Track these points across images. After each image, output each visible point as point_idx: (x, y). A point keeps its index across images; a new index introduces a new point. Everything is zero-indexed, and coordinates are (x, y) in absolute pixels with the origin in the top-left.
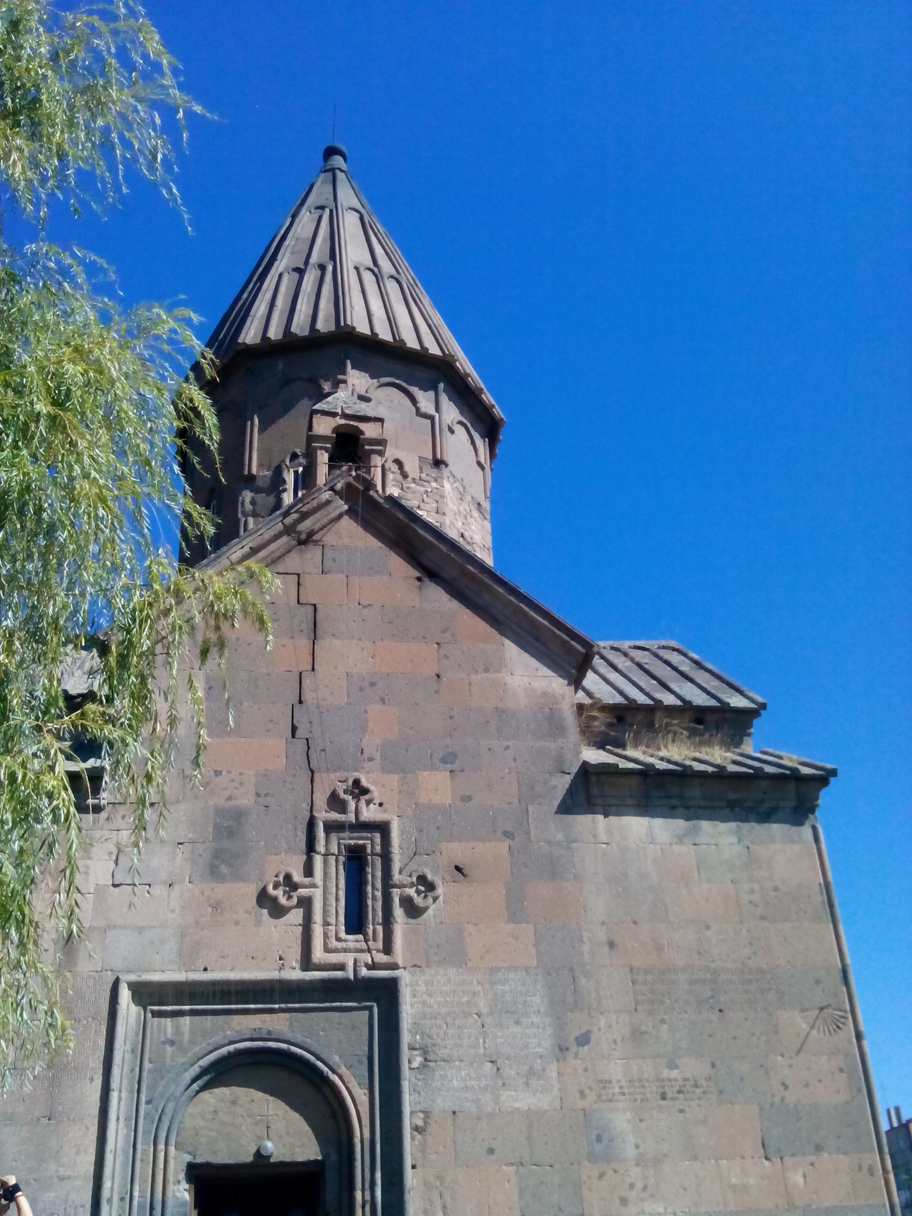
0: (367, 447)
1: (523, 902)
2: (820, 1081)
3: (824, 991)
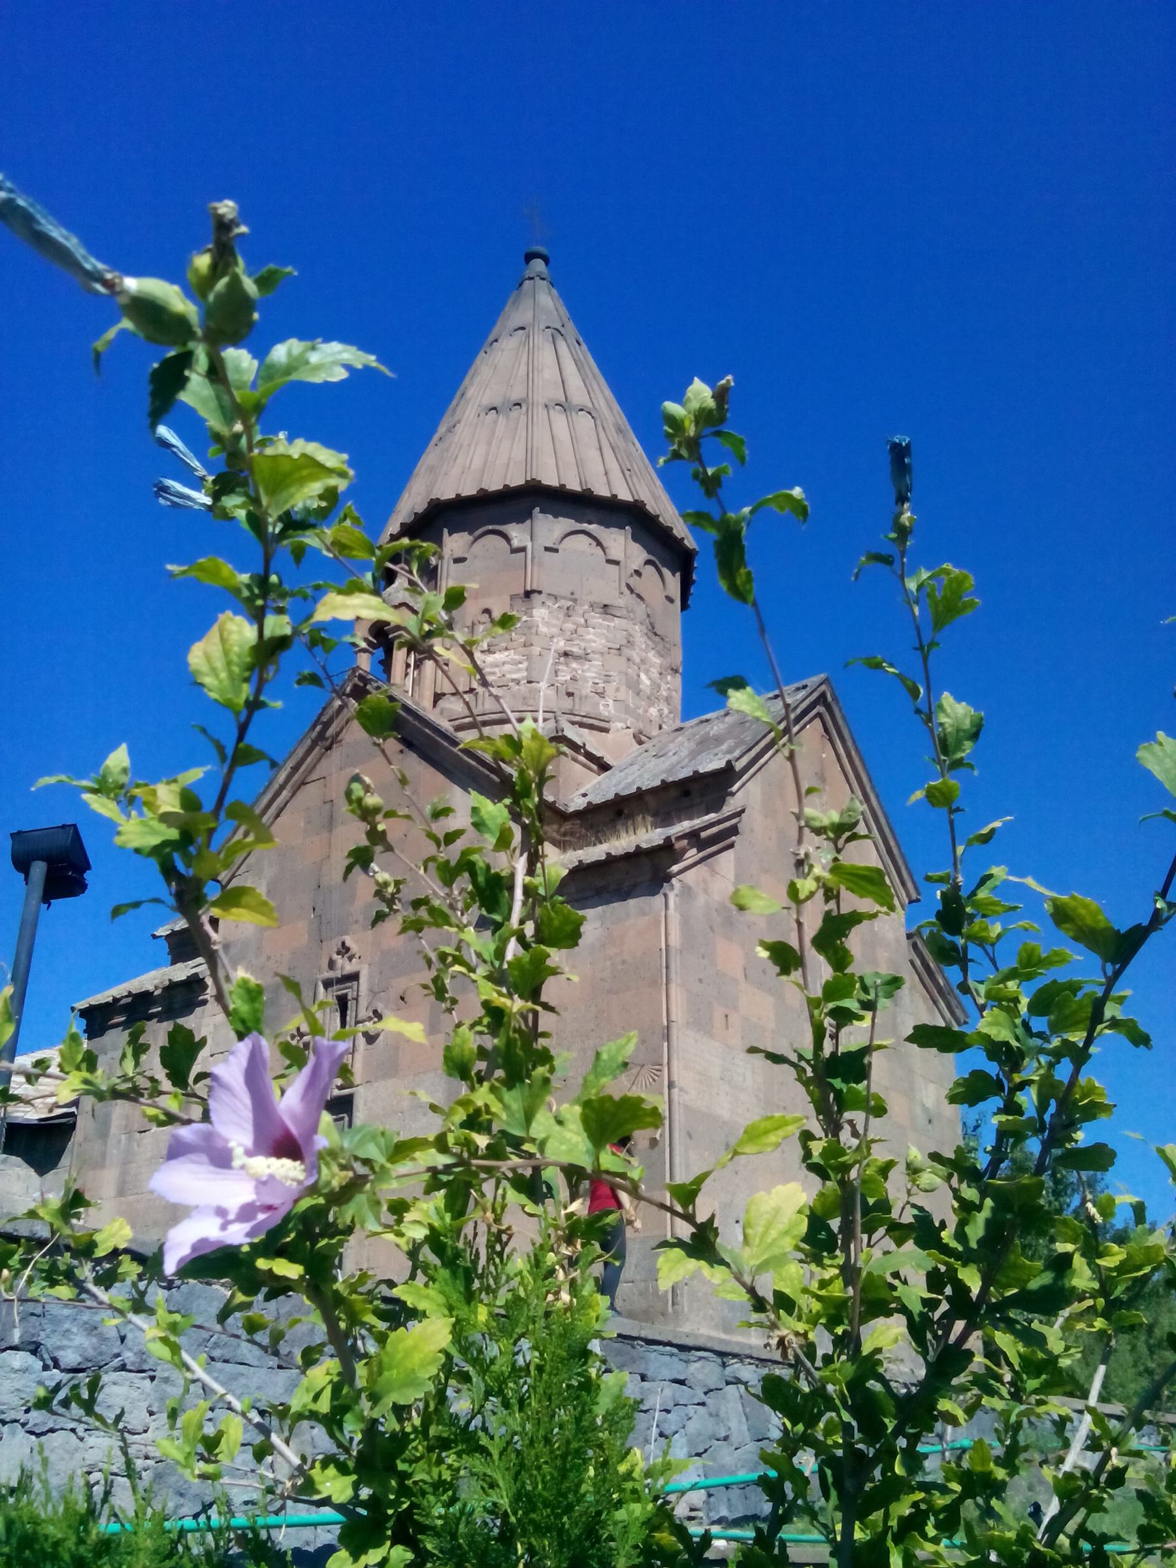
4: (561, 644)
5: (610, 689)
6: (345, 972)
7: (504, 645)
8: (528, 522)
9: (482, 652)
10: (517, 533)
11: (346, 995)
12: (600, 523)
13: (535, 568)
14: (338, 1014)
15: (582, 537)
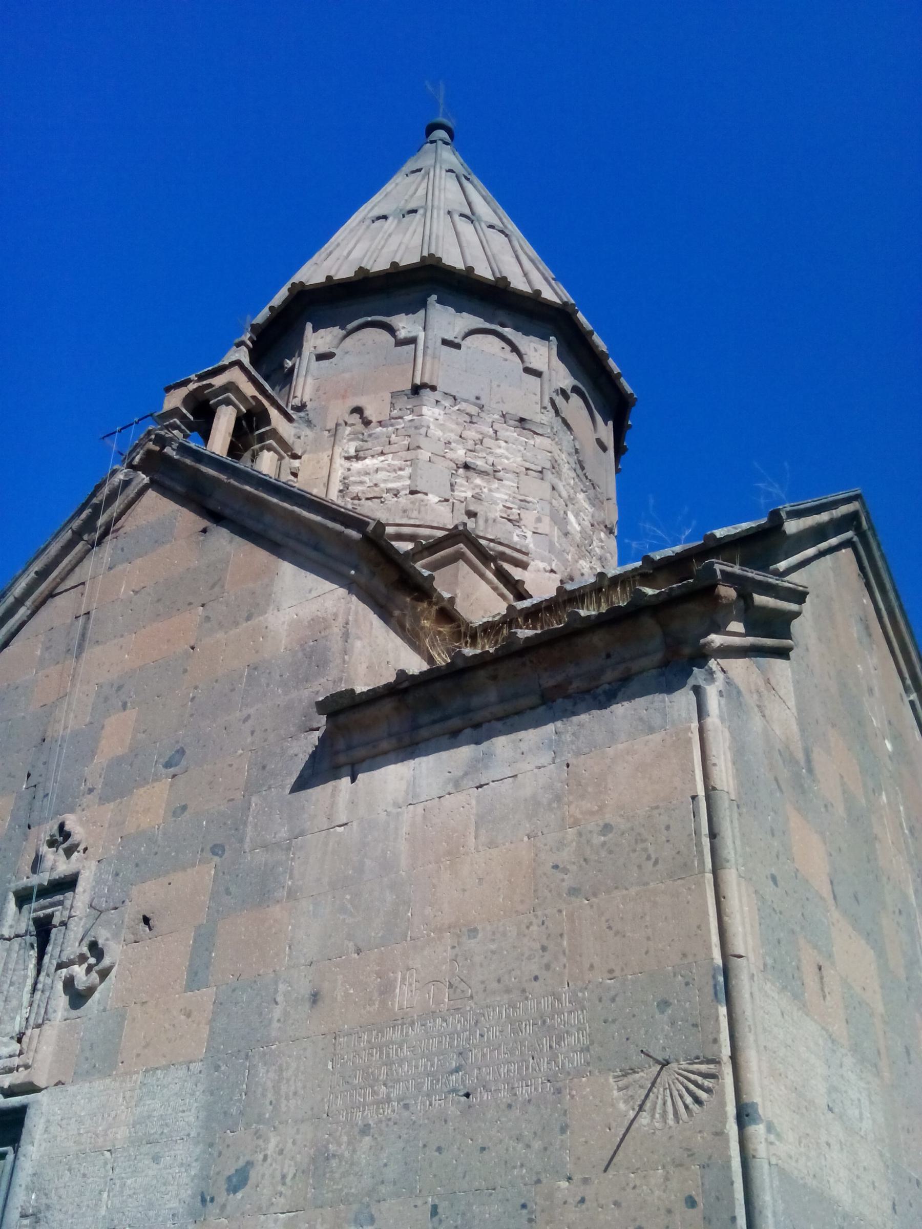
1: (211, 953)
3: (673, 1023)
4: (460, 453)
5: (528, 518)
6: (55, 876)
7: (379, 449)
8: (421, 313)
9: (348, 458)
10: (405, 325)
11: (51, 916)
12: (517, 329)
13: (428, 358)
14: (34, 953)
15: (491, 338)
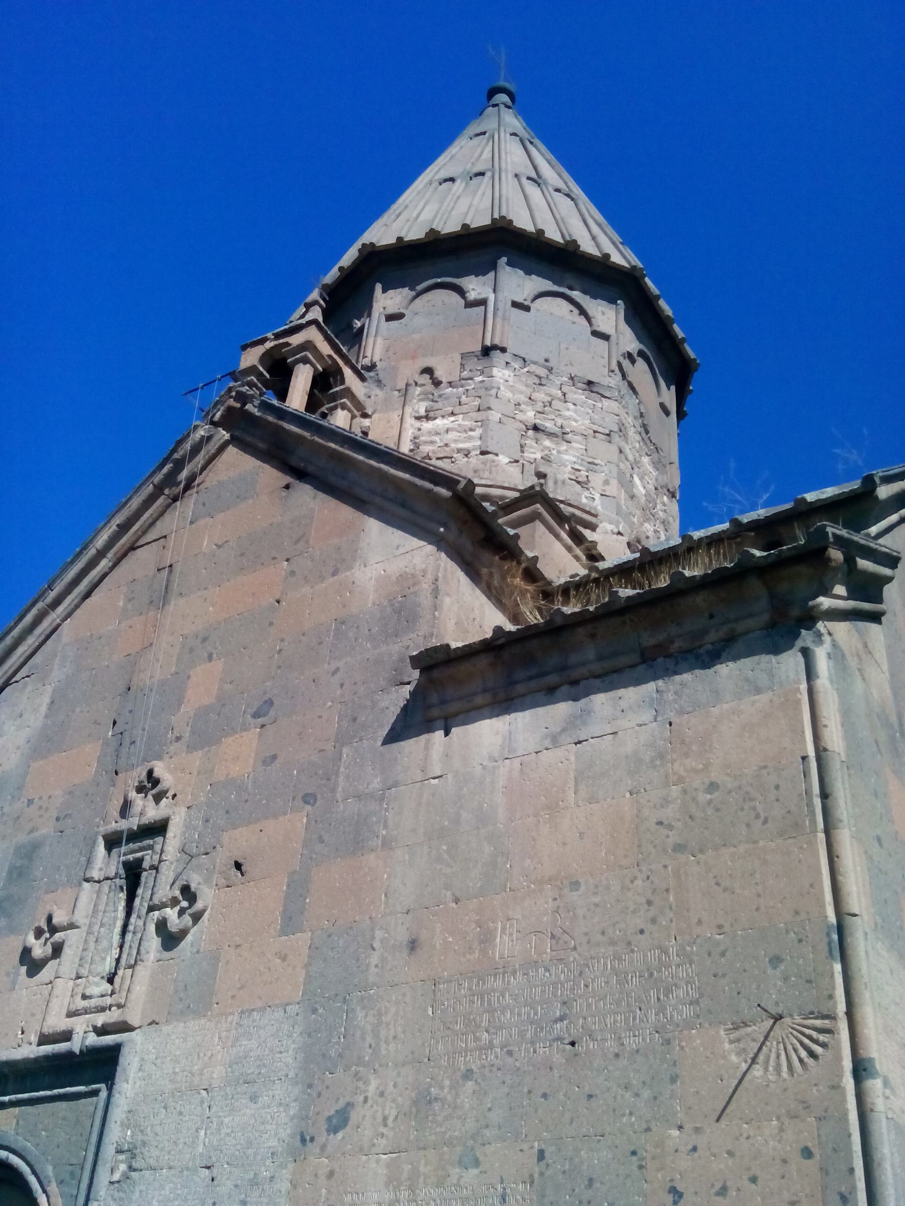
0: (289, 361)
1: (305, 899)
2: (754, 1180)
3: (786, 979)
4: (530, 415)
5: (597, 480)
6: (145, 820)
7: (450, 409)
8: (491, 275)
9: (418, 418)
10: (476, 287)
11: (140, 861)
12: (585, 292)
13: (499, 320)
14: (123, 896)
15: (559, 301)
